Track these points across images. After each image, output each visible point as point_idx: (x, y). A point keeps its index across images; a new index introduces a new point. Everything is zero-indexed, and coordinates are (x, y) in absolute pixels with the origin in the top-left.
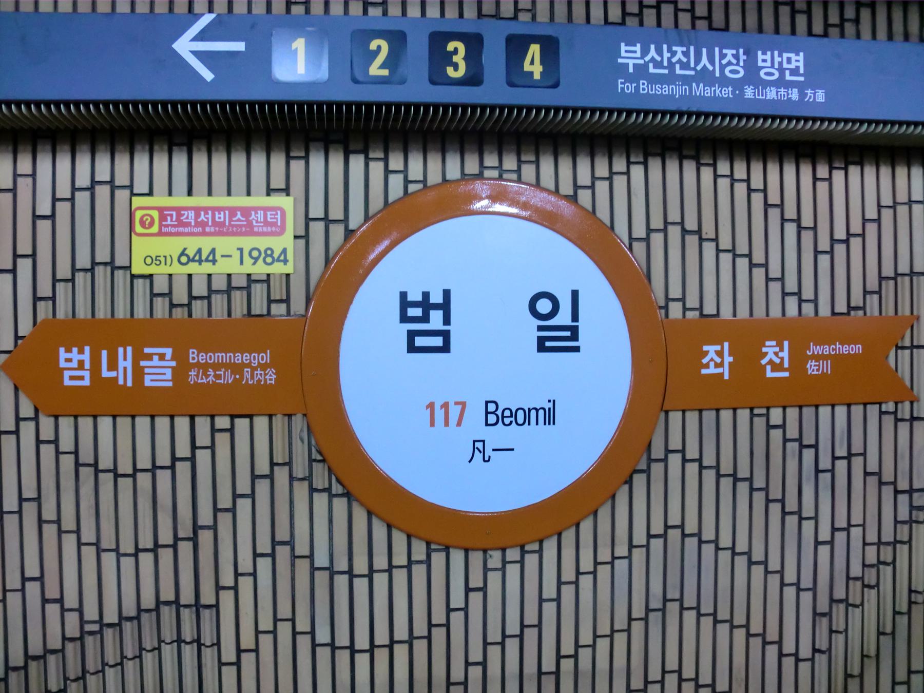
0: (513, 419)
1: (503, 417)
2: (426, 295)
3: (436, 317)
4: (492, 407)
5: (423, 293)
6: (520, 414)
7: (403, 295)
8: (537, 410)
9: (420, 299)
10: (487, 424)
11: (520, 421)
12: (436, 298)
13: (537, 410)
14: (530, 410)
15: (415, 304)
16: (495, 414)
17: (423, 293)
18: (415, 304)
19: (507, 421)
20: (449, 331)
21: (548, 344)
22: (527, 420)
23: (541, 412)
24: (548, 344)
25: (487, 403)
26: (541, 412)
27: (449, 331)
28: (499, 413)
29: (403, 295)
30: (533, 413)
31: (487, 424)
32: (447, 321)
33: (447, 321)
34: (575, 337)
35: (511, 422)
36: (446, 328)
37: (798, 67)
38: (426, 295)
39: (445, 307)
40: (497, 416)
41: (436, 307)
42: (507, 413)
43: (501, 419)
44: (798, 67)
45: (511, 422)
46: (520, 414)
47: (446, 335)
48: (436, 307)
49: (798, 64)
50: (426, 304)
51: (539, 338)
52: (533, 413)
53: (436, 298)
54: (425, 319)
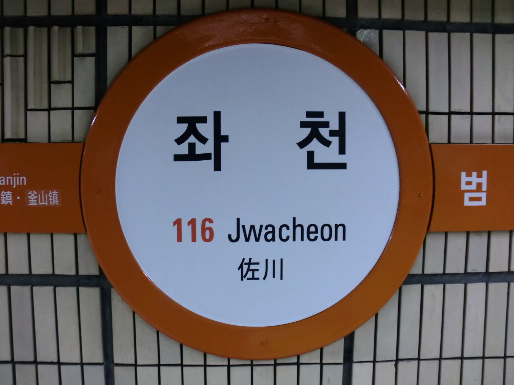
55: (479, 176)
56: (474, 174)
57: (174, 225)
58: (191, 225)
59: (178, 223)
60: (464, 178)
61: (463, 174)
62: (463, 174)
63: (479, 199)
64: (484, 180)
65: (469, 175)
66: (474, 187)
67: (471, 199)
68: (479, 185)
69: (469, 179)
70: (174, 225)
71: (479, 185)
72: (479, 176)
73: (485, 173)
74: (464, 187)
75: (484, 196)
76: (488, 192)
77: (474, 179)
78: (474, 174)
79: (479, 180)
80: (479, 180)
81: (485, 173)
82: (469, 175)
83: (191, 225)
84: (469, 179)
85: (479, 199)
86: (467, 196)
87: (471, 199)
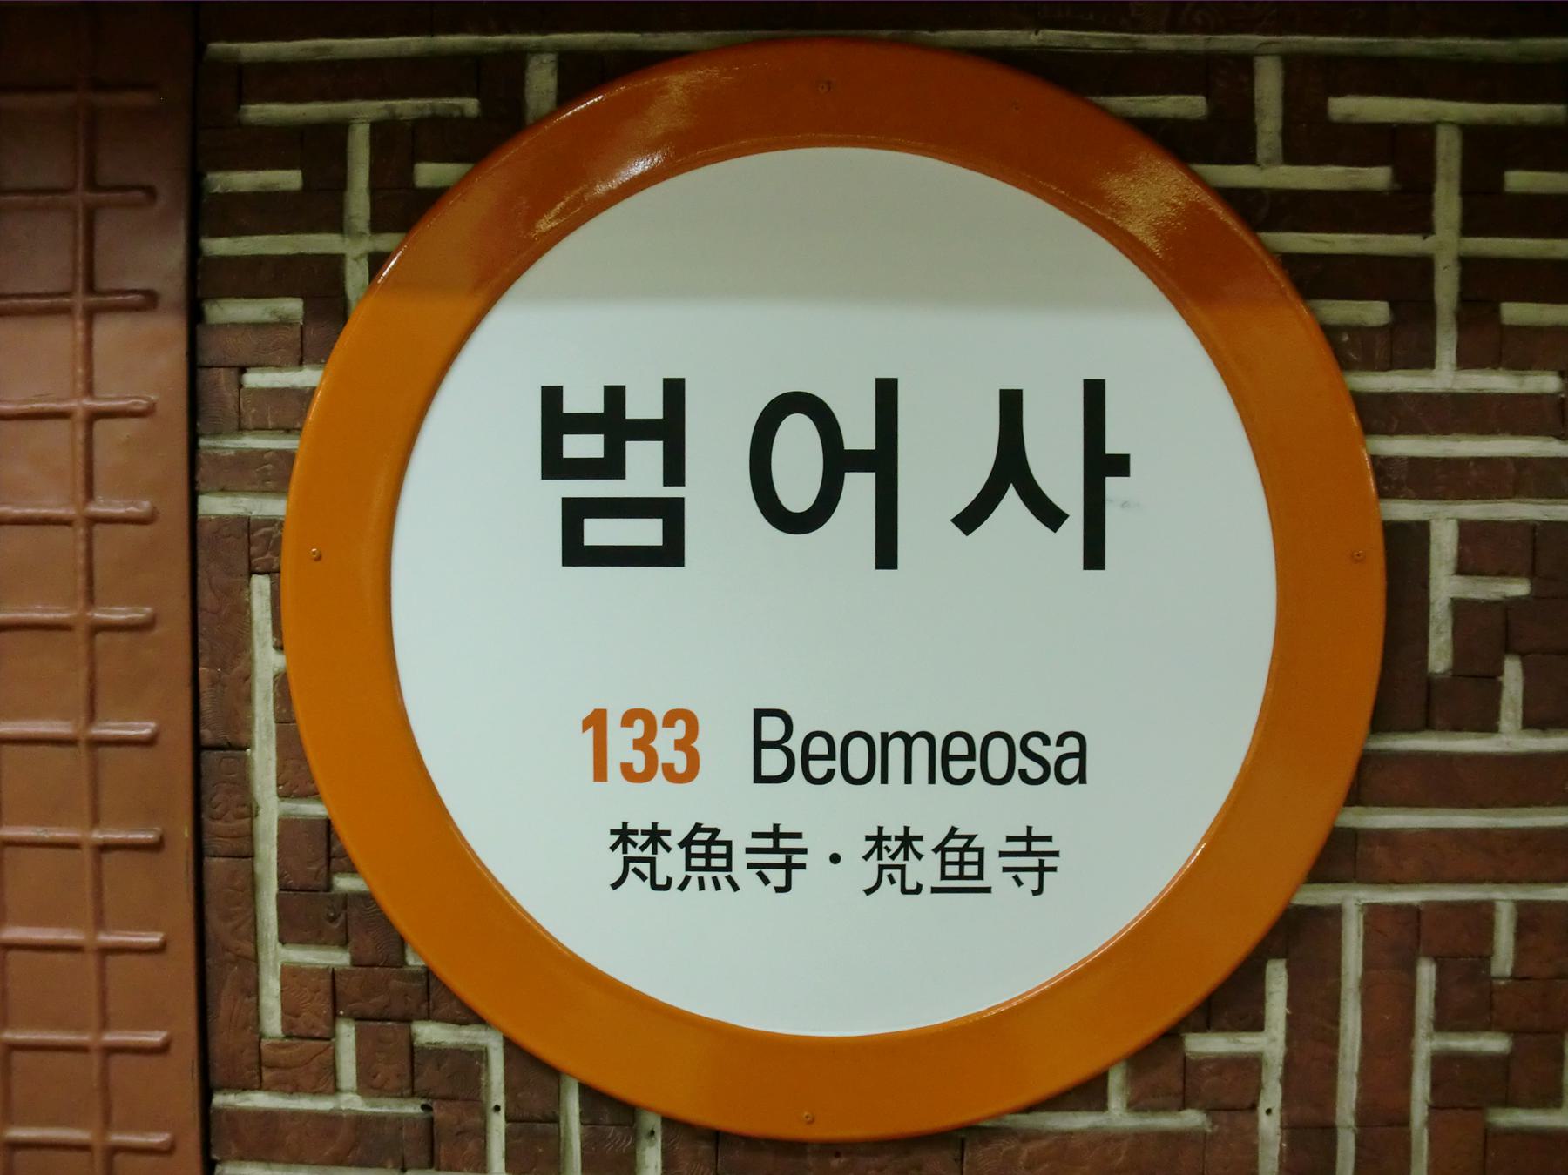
1: (807, 757)
2: (615, 395)
7: (552, 397)
8: (908, 740)
10: (759, 778)
11: (858, 770)
12: (645, 404)
13: (908, 740)
14: (886, 739)
15: (583, 423)
18: (583, 423)
19: (818, 768)
20: (679, 502)
22: (878, 767)
23: (920, 746)
26: (920, 746)
27: (679, 502)
29: (552, 397)
30: (897, 746)
31: (759, 778)
32: (674, 471)
33: (674, 471)
35: (831, 773)
36: (673, 492)
38: (615, 395)
39: (669, 430)
40: (789, 755)
41: (644, 430)
43: (799, 764)
45: (831, 773)
47: (671, 513)
48: (644, 430)
50: (613, 422)
52: (897, 746)
53: (645, 404)
54: (612, 466)
57: (585, 728)
58: (591, 730)
59: (596, 721)
70: (585, 728)
83: (591, 730)
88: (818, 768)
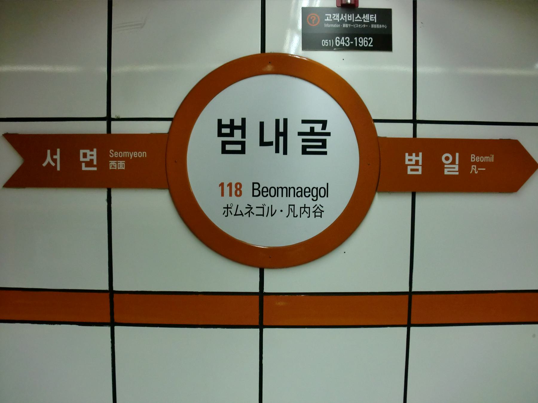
0: (268, 193)
1: (263, 192)
2: (232, 121)
3: (238, 134)
4: (256, 186)
5: (231, 120)
6: (273, 191)
7: (220, 121)
9: (229, 123)
11: (273, 194)
12: (238, 123)
15: (226, 126)
16: (259, 190)
17: (231, 120)
18: (226, 126)
19: (265, 194)
21: (308, 150)
22: (276, 194)
24: (308, 150)
25: (253, 183)
28: (260, 189)
29: (220, 121)
31: (253, 196)
32: (243, 136)
33: (243, 136)
34: (324, 146)
35: (267, 195)
36: (243, 140)
37: (92, 160)
38: (232, 121)
39: (243, 128)
40: (259, 191)
41: (238, 128)
42: (265, 190)
43: (261, 193)
44: (92, 160)
45: (267, 195)
46: (273, 191)
48: (238, 128)
49: (92, 158)
50: (232, 126)
51: (303, 146)
53: (238, 123)
55: (417, 155)
56: (414, 154)
60: (407, 157)
61: (407, 154)
62: (407, 154)
63: (417, 170)
64: (420, 158)
65: (410, 155)
66: (413, 162)
67: (412, 170)
68: (417, 162)
69: (410, 158)
71: (417, 162)
72: (417, 155)
73: (420, 154)
74: (407, 162)
75: (420, 168)
76: (423, 166)
77: (414, 157)
78: (414, 154)
79: (417, 158)
80: (417, 158)
81: (420, 154)
82: (410, 155)
84: (410, 158)
85: (417, 170)
86: (409, 168)
87: (412, 170)
88: (265, 194)
